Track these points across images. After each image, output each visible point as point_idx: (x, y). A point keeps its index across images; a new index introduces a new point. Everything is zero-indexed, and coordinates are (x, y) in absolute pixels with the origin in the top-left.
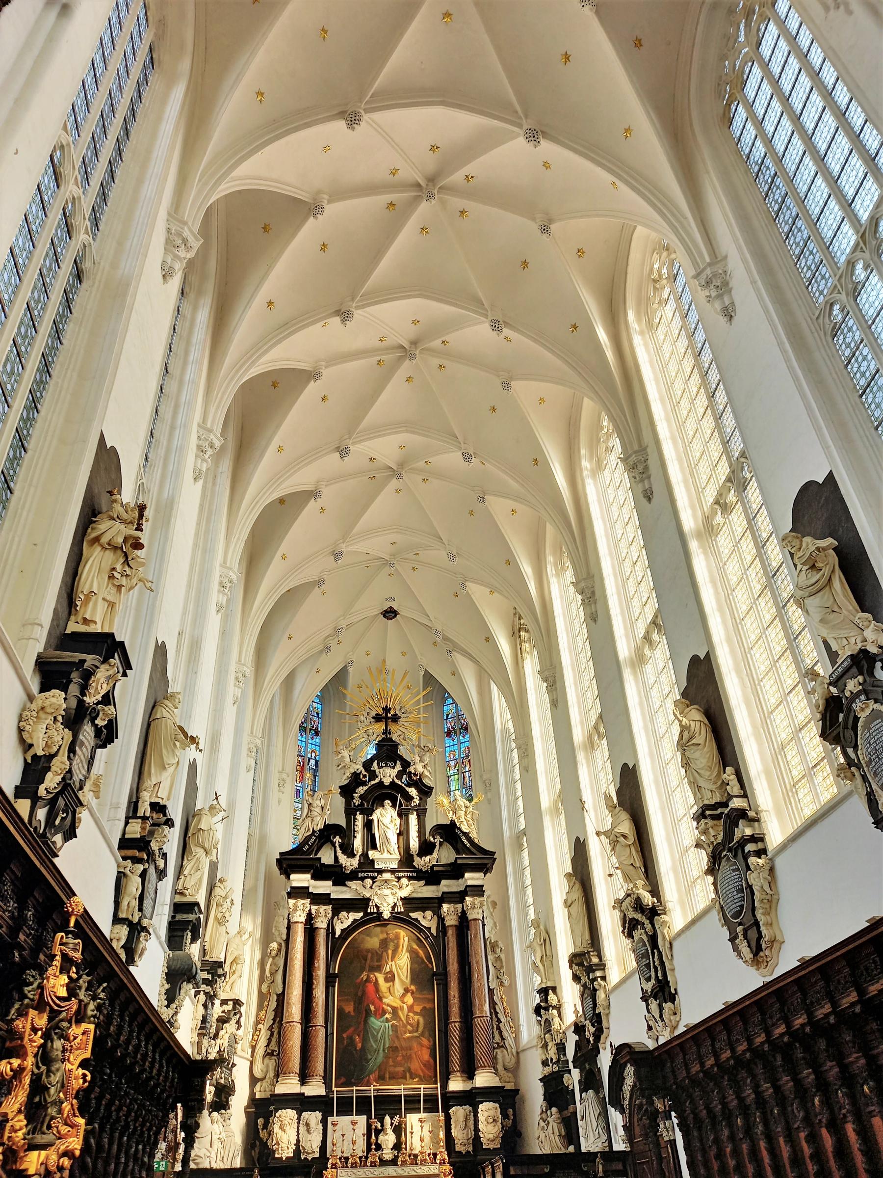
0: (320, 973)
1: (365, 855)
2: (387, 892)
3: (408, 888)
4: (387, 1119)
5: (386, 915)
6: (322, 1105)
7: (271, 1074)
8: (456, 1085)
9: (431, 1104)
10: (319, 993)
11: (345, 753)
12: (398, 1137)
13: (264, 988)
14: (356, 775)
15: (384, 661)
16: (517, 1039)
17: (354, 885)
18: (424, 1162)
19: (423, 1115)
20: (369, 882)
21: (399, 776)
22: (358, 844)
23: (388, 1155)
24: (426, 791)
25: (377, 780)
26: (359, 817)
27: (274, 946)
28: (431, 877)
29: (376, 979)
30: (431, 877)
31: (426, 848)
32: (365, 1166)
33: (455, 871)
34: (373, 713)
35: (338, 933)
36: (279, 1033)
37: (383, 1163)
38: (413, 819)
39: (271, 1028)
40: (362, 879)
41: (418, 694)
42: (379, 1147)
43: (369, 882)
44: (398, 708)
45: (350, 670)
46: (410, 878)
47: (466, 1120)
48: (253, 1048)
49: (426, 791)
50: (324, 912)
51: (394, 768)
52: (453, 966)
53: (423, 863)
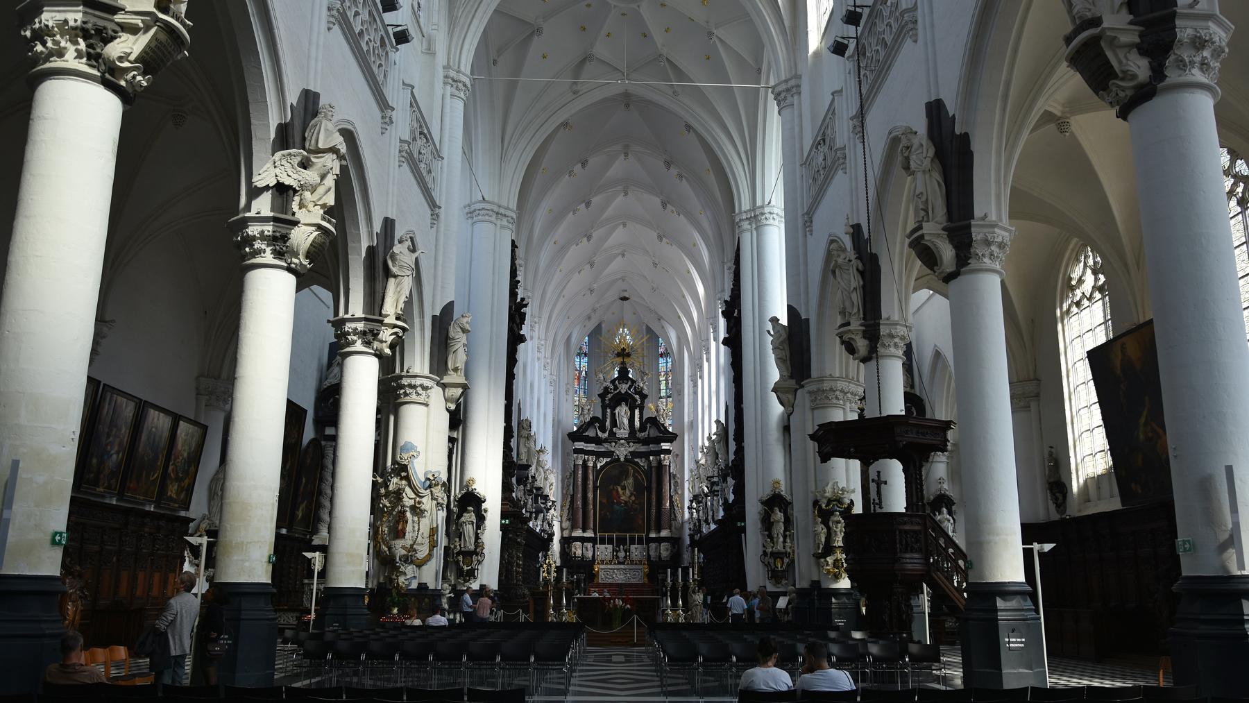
0: (591, 486)
1: (611, 431)
2: (622, 449)
3: (633, 447)
4: (622, 547)
5: (622, 459)
6: (593, 540)
7: (570, 527)
8: (653, 535)
9: (640, 542)
10: (590, 495)
11: (601, 376)
12: (626, 554)
13: (564, 492)
14: (606, 388)
15: (623, 318)
16: (683, 517)
17: (606, 445)
18: (636, 564)
19: (636, 546)
20: (614, 444)
21: (629, 388)
22: (608, 424)
23: (621, 559)
24: (644, 397)
25: (618, 391)
26: (609, 410)
27: (568, 474)
28: (645, 442)
29: (617, 490)
30: (645, 442)
31: (643, 428)
32: (611, 564)
33: (658, 441)
34: (616, 352)
35: (599, 467)
36: (572, 512)
37: (619, 563)
38: (637, 412)
39: (568, 509)
40: (610, 443)
41: (643, 338)
42: (617, 557)
43: (614, 444)
44: (630, 348)
45: (603, 326)
46: (634, 443)
47: (656, 548)
48: (561, 517)
49: (644, 397)
50: (592, 458)
51: (627, 384)
52: (654, 485)
53: (641, 435)
